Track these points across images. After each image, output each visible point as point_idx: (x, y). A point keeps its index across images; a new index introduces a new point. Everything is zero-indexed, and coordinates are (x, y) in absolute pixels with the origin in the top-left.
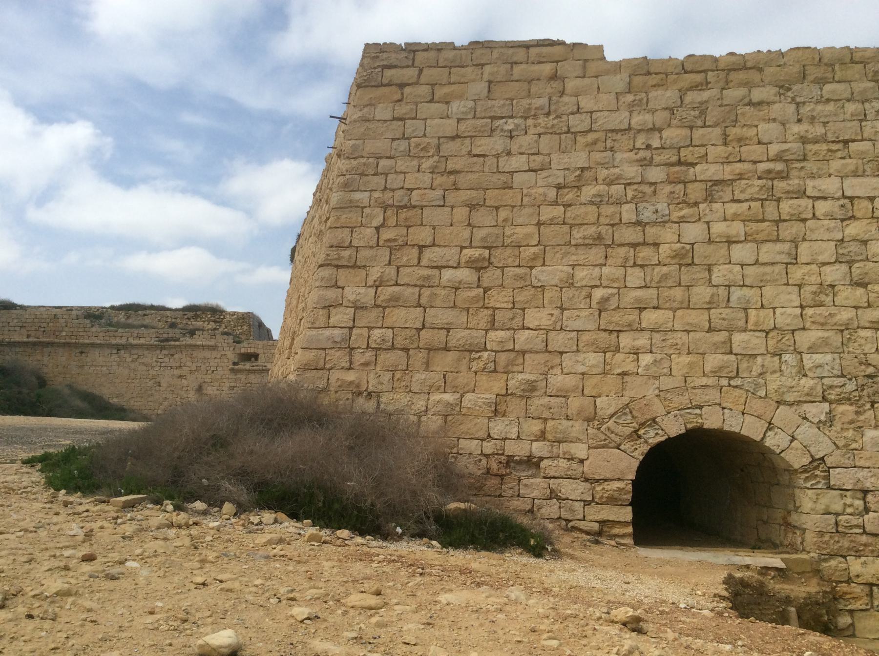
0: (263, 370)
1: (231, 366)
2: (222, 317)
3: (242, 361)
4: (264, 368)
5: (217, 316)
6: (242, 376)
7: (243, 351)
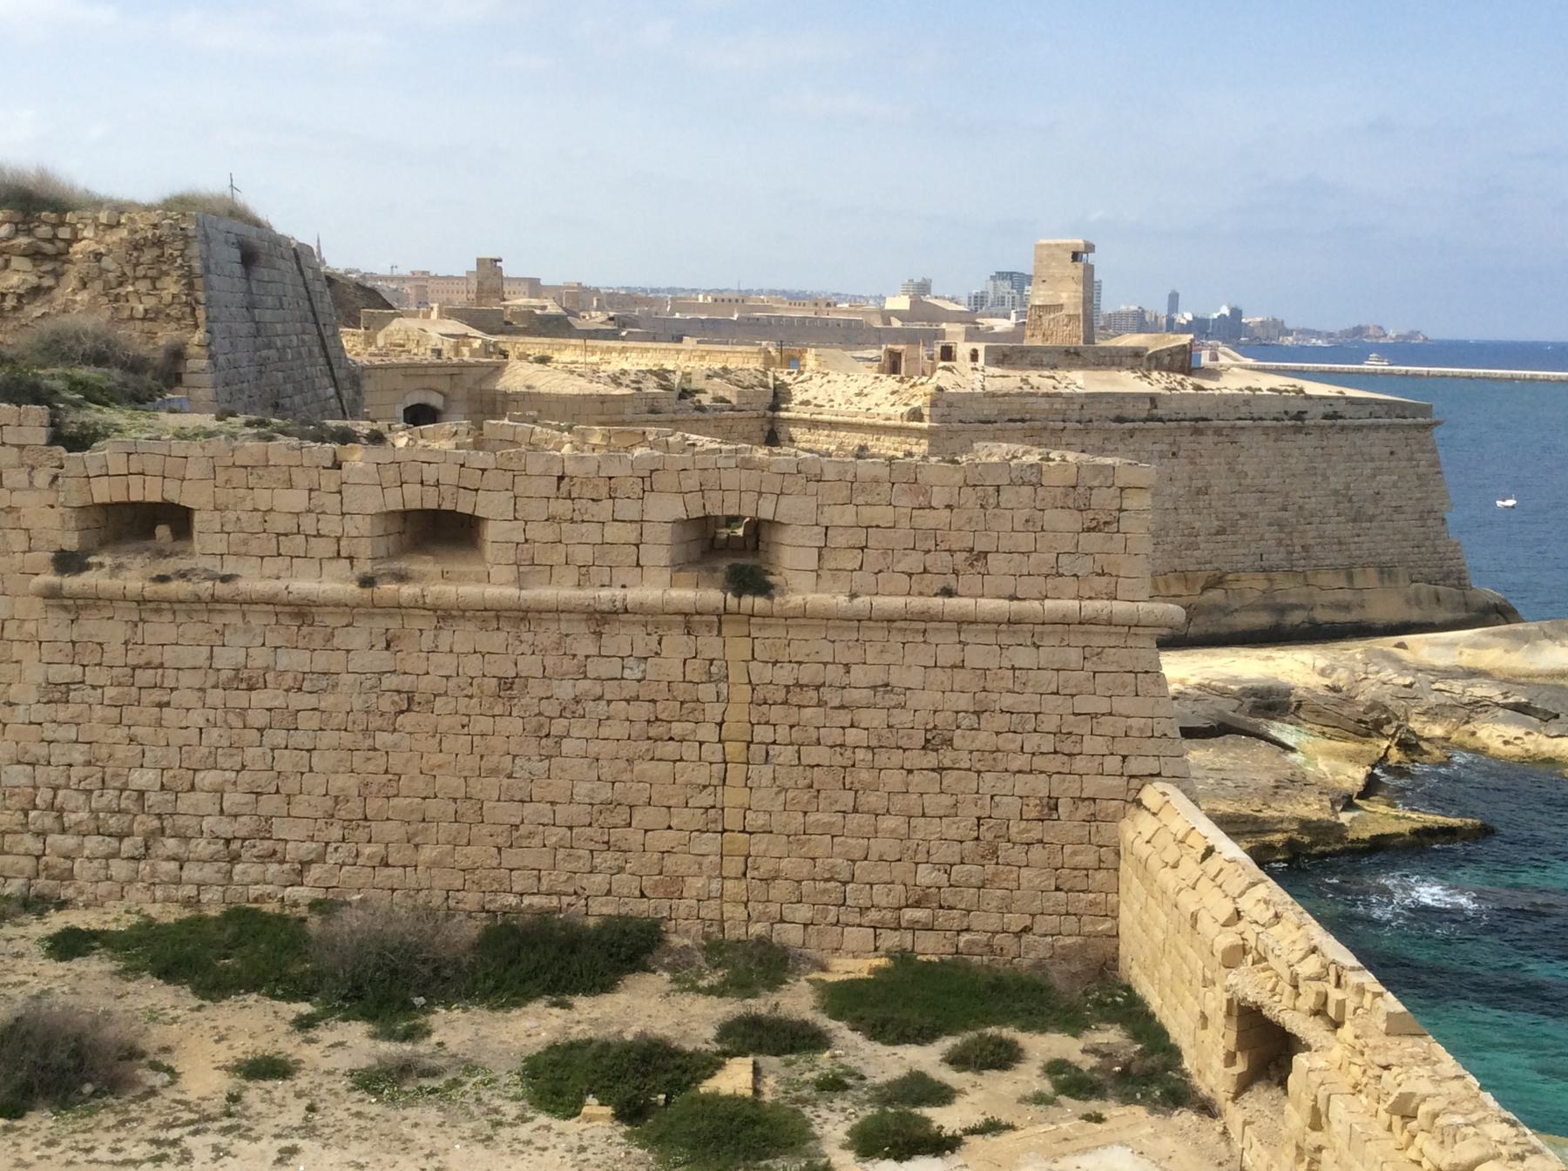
0: (215, 599)
1: (50, 578)
2: (64, 233)
3: (103, 545)
4: (222, 589)
5: (44, 231)
6: (110, 631)
7: (103, 492)
